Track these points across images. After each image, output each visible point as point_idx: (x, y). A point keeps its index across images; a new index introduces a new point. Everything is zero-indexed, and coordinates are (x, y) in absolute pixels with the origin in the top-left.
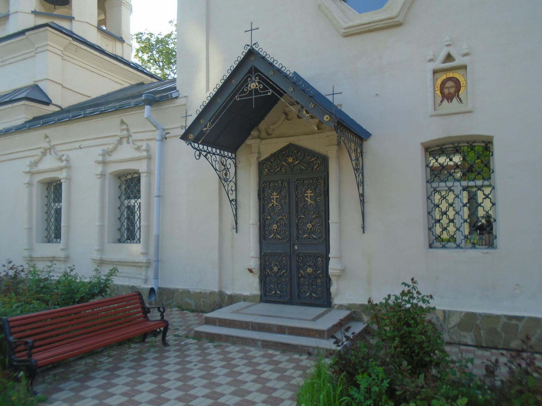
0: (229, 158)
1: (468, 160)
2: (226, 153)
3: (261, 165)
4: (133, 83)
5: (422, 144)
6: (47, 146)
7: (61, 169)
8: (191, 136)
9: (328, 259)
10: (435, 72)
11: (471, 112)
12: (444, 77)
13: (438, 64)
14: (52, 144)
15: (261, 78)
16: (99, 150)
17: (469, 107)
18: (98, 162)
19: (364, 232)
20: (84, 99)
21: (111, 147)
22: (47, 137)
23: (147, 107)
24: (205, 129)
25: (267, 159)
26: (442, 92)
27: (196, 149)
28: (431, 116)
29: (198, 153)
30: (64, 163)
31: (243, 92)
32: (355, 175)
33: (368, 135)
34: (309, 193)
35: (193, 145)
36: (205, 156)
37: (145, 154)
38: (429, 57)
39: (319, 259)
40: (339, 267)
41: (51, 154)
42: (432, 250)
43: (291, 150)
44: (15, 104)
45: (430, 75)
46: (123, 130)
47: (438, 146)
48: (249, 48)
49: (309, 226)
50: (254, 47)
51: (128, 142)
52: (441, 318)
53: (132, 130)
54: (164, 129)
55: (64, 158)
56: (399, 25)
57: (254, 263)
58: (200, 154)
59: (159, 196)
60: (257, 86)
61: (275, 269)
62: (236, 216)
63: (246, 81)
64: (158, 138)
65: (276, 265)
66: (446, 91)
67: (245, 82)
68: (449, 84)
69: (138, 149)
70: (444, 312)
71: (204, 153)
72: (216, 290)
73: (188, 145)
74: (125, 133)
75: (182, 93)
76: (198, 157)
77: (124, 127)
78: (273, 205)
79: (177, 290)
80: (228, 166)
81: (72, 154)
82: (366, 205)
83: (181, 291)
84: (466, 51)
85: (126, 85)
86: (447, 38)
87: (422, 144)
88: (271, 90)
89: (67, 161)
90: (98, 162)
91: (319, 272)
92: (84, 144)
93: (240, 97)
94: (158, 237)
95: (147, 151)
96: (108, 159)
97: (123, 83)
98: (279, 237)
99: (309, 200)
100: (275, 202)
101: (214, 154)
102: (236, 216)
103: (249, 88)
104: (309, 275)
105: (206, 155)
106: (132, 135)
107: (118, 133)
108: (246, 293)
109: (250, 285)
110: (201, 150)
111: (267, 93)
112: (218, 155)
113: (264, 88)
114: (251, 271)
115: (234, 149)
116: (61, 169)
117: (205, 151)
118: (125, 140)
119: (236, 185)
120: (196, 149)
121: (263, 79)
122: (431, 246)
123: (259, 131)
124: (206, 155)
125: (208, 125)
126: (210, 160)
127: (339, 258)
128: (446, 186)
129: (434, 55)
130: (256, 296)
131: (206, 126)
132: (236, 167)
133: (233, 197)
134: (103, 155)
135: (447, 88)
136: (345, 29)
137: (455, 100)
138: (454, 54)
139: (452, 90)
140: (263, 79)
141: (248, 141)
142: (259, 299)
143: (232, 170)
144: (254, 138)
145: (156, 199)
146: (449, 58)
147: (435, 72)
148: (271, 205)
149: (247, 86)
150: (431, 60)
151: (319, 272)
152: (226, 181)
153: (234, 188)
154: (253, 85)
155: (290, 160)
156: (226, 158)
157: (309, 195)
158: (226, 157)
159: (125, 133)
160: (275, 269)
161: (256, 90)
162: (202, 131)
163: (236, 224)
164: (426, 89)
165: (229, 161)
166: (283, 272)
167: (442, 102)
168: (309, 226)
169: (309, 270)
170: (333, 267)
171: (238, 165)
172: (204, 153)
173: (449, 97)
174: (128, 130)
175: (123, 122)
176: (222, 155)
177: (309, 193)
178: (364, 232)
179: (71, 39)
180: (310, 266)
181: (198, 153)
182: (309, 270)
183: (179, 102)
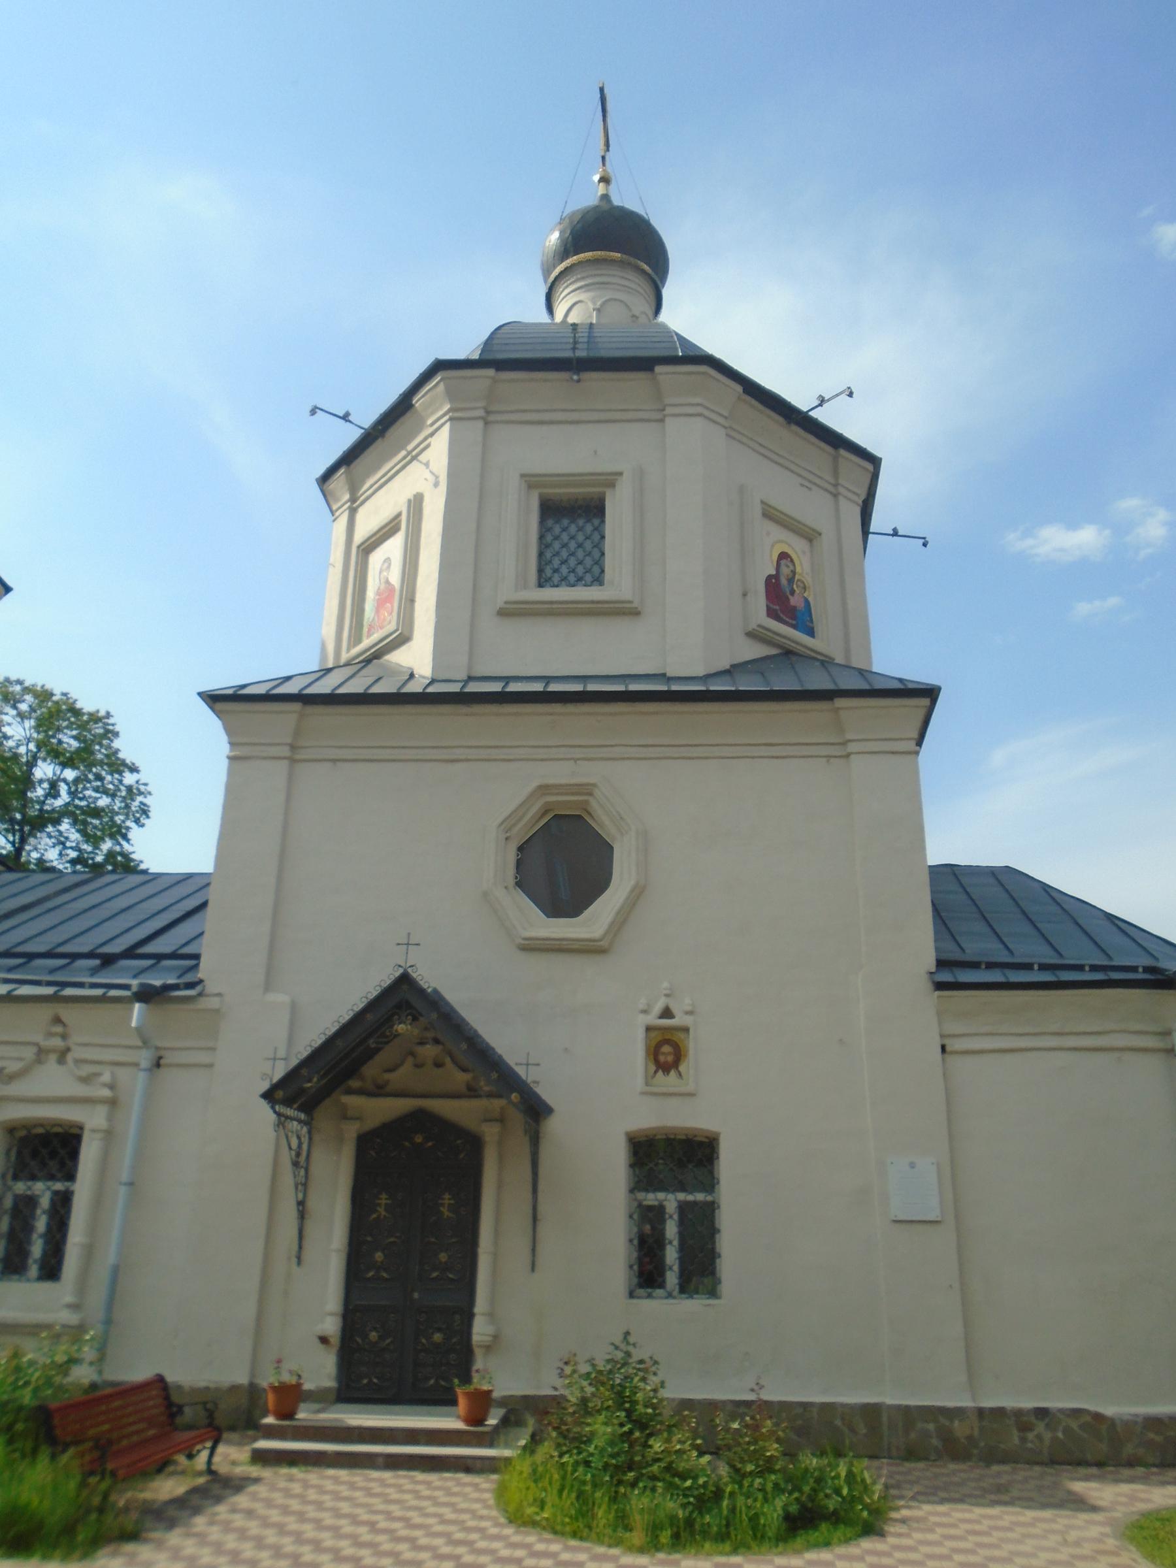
3: (364, 1142)
10: (649, 1029)
11: (691, 1095)
13: (652, 1019)
17: (690, 1088)
23: (137, 1006)
26: (656, 1061)
33: (549, 1110)
34: (447, 1199)
37: (106, 1093)
38: (641, 1007)
39: (457, 1317)
40: (490, 1330)
42: (635, 1301)
43: (420, 1120)
45: (640, 1034)
49: (443, 1257)
50: (410, 970)
53: (75, 1039)
54: (157, 1048)
56: (602, 951)
57: (331, 1326)
61: (373, 1336)
64: (144, 1064)
66: (662, 1058)
68: (666, 1049)
69: (85, 1080)
72: (242, 1379)
74: (57, 1042)
75: (211, 987)
77: (59, 1029)
78: (379, 1217)
84: (689, 1008)
86: (666, 985)
91: (454, 1340)
94: (116, 1270)
95: (111, 1087)
98: (385, 1275)
106: (73, 1047)
107: (39, 1038)
109: (320, 1370)
114: (324, 1340)
118: (53, 1058)
122: (631, 1295)
125: (315, 1079)
127: (491, 1315)
129: (648, 1005)
131: (310, 1081)
135: (664, 1054)
137: (673, 1073)
138: (675, 1009)
139: (670, 1059)
145: (123, 1190)
146: (667, 1013)
147: (649, 1029)
148: (374, 1216)
150: (645, 1012)
151: (454, 1340)
155: (419, 1139)
157: (447, 1202)
160: (373, 1336)
163: (300, 1247)
166: (388, 1341)
167: (656, 1072)
168: (443, 1257)
169: (438, 1337)
170: (480, 1330)
173: (665, 1068)
175: (58, 1020)
177: (447, 1199)
180: (439, 1330)
182: (438, 1337)
183: (204, 1003)
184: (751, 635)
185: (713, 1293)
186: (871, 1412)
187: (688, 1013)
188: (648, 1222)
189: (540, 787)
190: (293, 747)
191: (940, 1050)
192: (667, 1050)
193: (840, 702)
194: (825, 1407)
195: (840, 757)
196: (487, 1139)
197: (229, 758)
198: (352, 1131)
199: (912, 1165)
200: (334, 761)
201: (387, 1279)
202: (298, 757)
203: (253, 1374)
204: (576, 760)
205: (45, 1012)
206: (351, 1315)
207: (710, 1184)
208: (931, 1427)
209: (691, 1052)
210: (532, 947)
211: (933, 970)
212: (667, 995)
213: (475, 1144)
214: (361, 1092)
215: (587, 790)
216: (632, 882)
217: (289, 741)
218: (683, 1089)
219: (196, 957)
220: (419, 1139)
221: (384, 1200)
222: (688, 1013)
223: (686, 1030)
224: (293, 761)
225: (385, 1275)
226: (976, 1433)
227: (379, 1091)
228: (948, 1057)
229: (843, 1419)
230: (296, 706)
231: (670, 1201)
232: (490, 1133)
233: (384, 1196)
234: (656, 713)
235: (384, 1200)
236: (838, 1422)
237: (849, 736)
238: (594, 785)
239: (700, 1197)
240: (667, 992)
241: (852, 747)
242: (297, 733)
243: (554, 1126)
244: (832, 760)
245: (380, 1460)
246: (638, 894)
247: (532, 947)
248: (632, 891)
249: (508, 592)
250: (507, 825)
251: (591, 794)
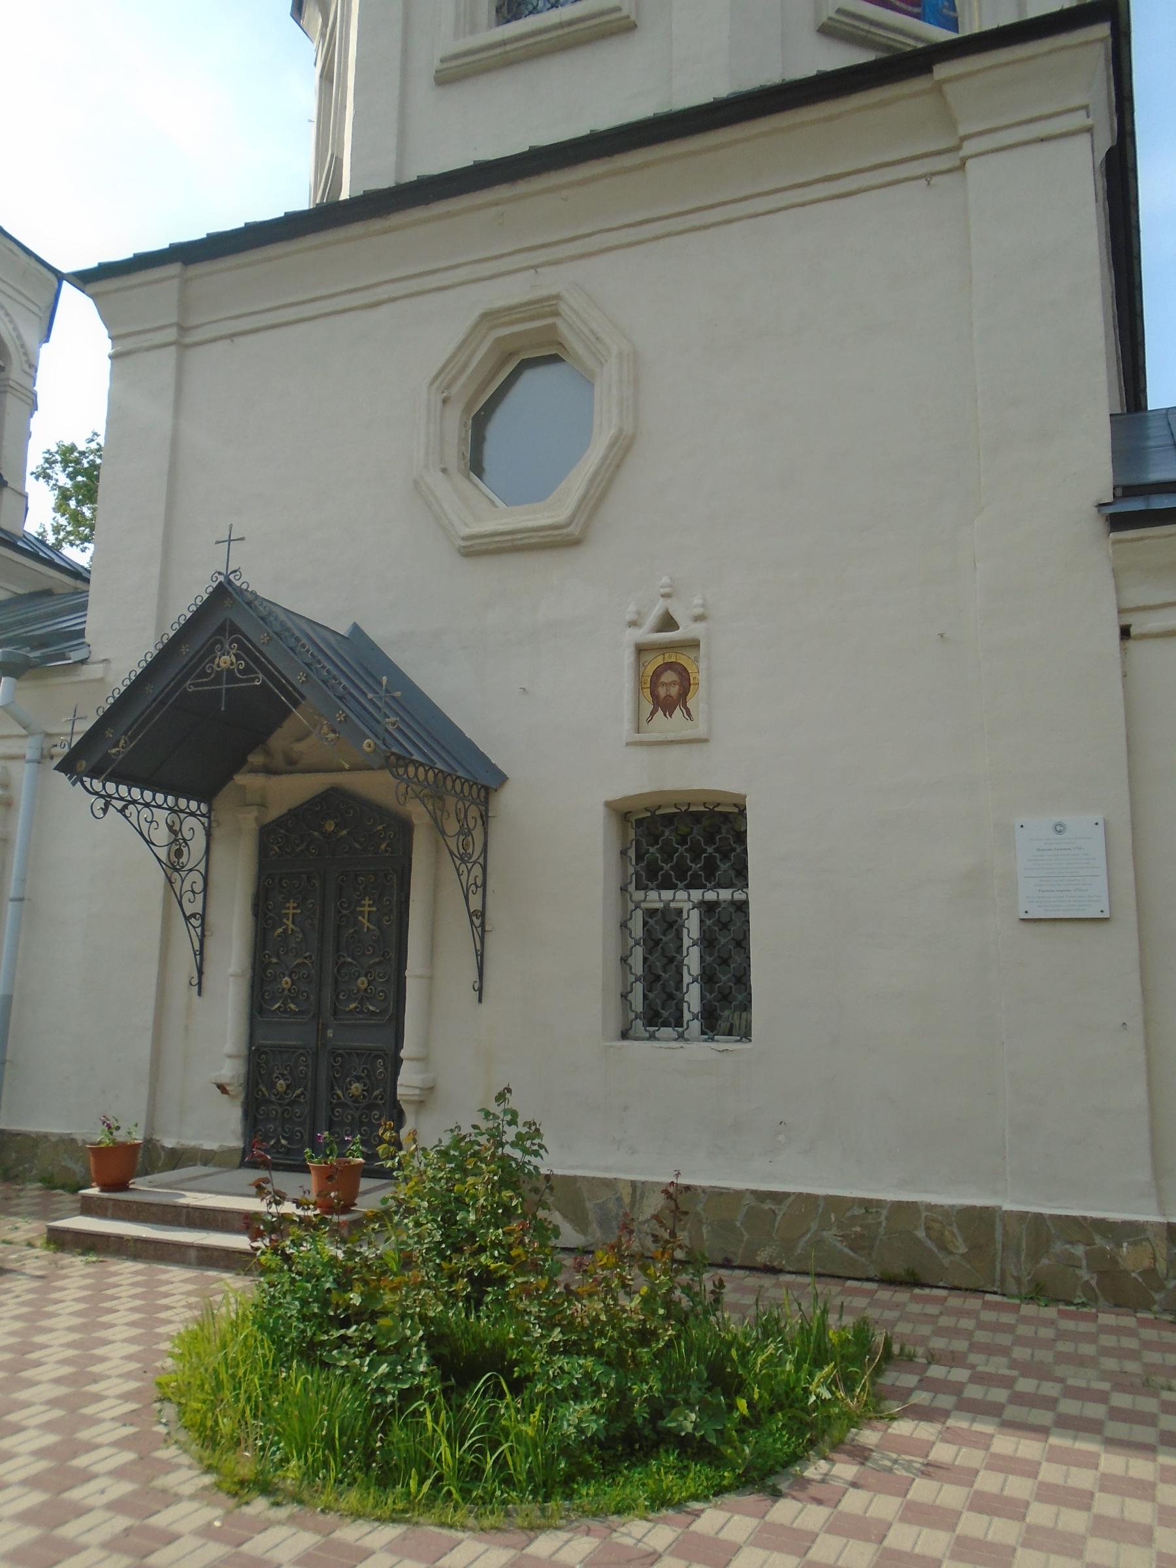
0: (192, 814)
1: (686, 845)
2: (183, 803)
3: (268, 835)
4: (21, 591)
5: (608, 804)
8: (83, 765)
9: (397, 1063)
10: (641, 650)
11: (705, 741)
12: (659, 661)
15: (242, 647)
17: (700, 730)
19: (480, 1000)
24: (114, 751)
25: (279, 822)
26: (654, 694)
27: (96, 793)
28: (628, 744)
29: (101, 803)
31: (203, 674)
32: (458, 870)
33: (502, 779)
34: (367, 906)
35: (88, 785)
36: (122, 811)
38: (629, 617)
42: (626, 1043)
43: (333, 802)
45: (628, 657)
47: (647, 810)
48: (221, 578)
50: (231, 577)
52: (627, 1200)
54: (48, 735)
56: (574, 543)
57: (231, 1070)
58: (107, 804)
59: (21, 900)
60: (232, 664)
61: (281, 1084)
62: (201, 953)
63: (211, 651)
65: (283, 1075)
66: (662, 692)
67: (209, 652)
68: (669, 676)
70: (633, 1184)
71: (119, 804)
73: (74, 784)
76: (100, 814)
78: (285, 931)
79: (46, 1136)
80: (187, 834)
82: (489, 939)
83: (53, 1139)
86: (665, 580)
87: (608, 804)
88: (261, 676)
91: (376, 1093)
93: (195, 685)
98: (292, 1006)
99: (365, 921)
100: (289, 923)
101: (147, 805)
102: (201, 953)
103: (215, 666)
104: (355, 1099)
105: (125, 807)
109: (221, 1125)
110: (110, 796)
111: (253, 680)
112: (159, 807)
113: (247, 670)
115: (207, 794)
117: (122, 799)
119: (206, 879)
120: (96, 793)
121: (246, 650)
122: (625, 1035)
123: (268, 753)
124: (125, 807)
125: (122, 742)
126: (134, 819)
127: (423, 1060)
128: (661, 900)
129: (639, 613)
130: (232, 1150)
131: (116, 745)
132: (209, 835)
133: (197, 907)
135: (664, 684)
136: (465, 539)
139: (674, 691)
140: (246, 650)
141: (240, 779)
142: (238, 1159)
143: (198, 844)
144: (254, 770)
145: (11, 907)
146: (668, 623)
147: (641, 650)
149: (212, 661)
150: (633, 624)
151: (376, 1093)
152: (177, 870)
153: (199, 887)
154: (225, 661)
156: (182, 816)
158: (182, 811)
160: (281, 1084)
161: (230, 672)
162: (107, 754)
163: (200, 972)
164: (617, 683)
165: (191, 821)
166: (298, 1092)
167: (653, 714)
168: (362, 982)
169: (356, 1088)
170: (408, 1081)
171: (216, 833)
172: (119, 804)
173: (666, 705)
176: (170, 809)
177: (367, 906)
178: (480, 1000)
180: (358, 1079)
181: (101, 803)
182: (356, 1088)
183: (88, 672)
184: (827, 31)
185: (746, 1035)
186: (978, 1220)
187: (699, 618)
188: (661, 931)
189: (484, 316)
190: (183, 329)
191: (1117, 632)
192: (667, 680)
193: (942, 71)
194: (900, 1208)
195: (949, 171)
196: (415, 821)
197: (111, 357)
198: (249, 821)
199: (1059, 829)
200: (232, 336)
201: (295, 1013)
202: (188, 340)
203: (150, 1125)
204: (535, 267)
206: (258, 1060)
207: (740, 875)
208: (1079, 1250)
209: (702, 677)
210: (478, 549)
211: (1109, 499)
212: (665, 596)
213: (405, 828)
214: (269, 771)
215: (549, 306)
216: (613, 431)
217: (174, 319)
218: (688, 733)
220: (330, 826)
221: (291, 909)
222: (699, 618)
223: (693, 644)
224: (182, 347)
225: (292, 1006)
226: (1162, 1266)
227: (292, 765)
228: (1130, 644)
229: (928, 1229)
230: (175, 269)
231: (685, 900)
232: (418, 813)
233: (292, 904)
234: (646, 165)
235: (291, 909)
236: (921, 1234)
237: (963, 131)
238: (557, 297)
239: (725, 894)
240: (667, 590)
241: (969, 148)
242: (184, 307)
243: (507, 801)
244: (935, 180)
245: (193, 1254)
246: (622, 450)
247: (478, 549)
248: (612, 445)
249: (443, 39)
250: (444, 379)
251: (556, 314)
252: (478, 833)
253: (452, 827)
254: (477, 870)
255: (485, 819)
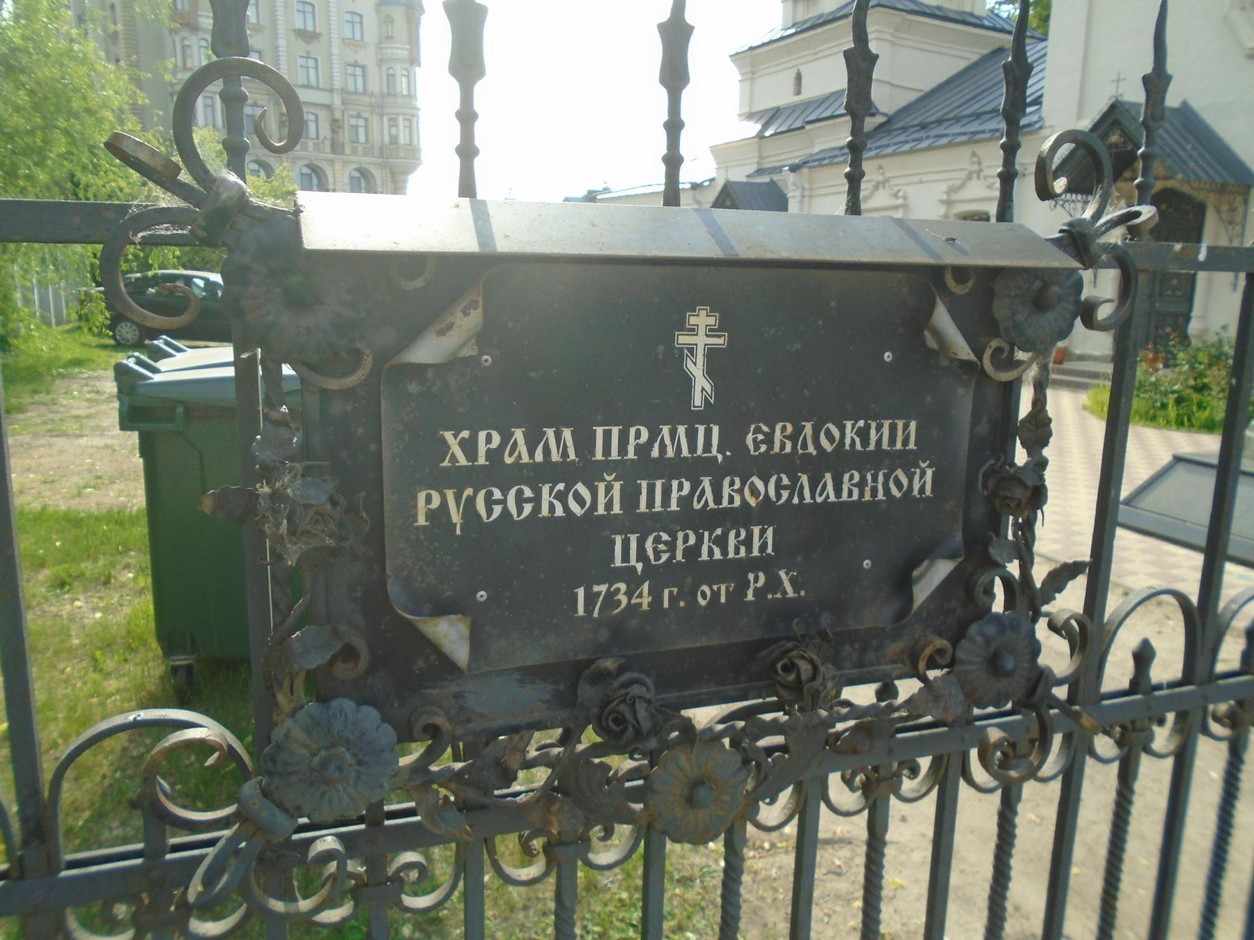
6: (881, 178)
7: (896, 208)
14: (887, 175)
16: (944, 187)
18: (943, 202)
20: (913, 96)
21: (958, 183)
22: (880, 168)
30: (900, 201)
41: (884, 187)
44: (838, 120)
46: (972, 163)
51: (979, 178)
53: (985, 164)
55: (901, 194)
74: (976, 167)
77: (975, 160)
81: (911, 191)
85: (975, 58)
89: (904, 198)
90: (943, 202)
92: (926, 178)
96: (955, 197)
97: (968, 55)
108: (1097, 353)
113: (1124, 143)
116: (896, 208)
118: (975, 176)
134: (948, 193)
140: (1124, 133)
159: (976, 167)
174: (979, 163)
175: (974, 154)
179: (904, 14)
205: (966, 151)
213: (1201, 209)
219: (1040, 103)
252: (1241, 210)
253: (1225, 208)
254: (1238, 228)
255: (1246, 202)
